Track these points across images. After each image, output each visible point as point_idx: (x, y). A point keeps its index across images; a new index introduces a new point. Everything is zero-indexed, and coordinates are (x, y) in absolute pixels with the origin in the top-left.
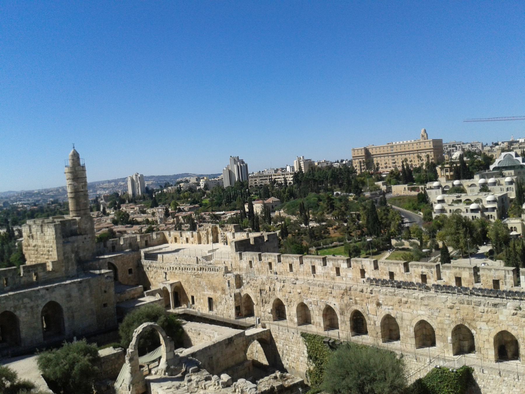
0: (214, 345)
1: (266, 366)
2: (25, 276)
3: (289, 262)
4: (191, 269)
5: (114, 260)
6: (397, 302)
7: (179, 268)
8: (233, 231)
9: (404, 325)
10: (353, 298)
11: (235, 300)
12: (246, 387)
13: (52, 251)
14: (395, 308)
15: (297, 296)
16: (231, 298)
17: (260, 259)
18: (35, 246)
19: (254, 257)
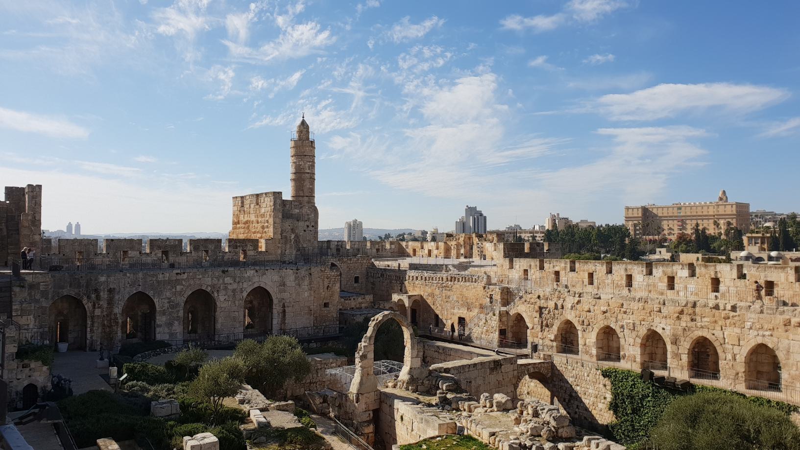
0: (475, 365)
1: (556, 397)
2: (230, 252)
3: (587, 270)
4: (438, 280)
5: (338, 262)
6: (782, 323)
7: (422, 277)
8: (495, 241)
9: (791, 361)
10: (698, 318)
11: (501, 320)
12: (542, 408)
13: (267, 227)
14: (775, 333)
15: (601, 317)
16: (495, 317)
17: (542, 268)
18: (246, 222)
19: (533, 264)
